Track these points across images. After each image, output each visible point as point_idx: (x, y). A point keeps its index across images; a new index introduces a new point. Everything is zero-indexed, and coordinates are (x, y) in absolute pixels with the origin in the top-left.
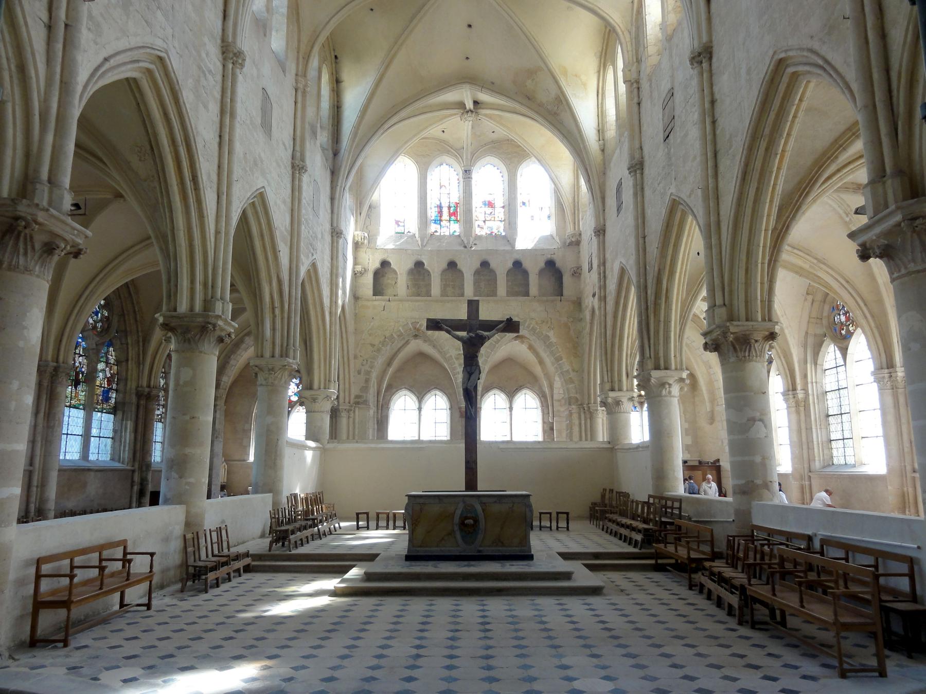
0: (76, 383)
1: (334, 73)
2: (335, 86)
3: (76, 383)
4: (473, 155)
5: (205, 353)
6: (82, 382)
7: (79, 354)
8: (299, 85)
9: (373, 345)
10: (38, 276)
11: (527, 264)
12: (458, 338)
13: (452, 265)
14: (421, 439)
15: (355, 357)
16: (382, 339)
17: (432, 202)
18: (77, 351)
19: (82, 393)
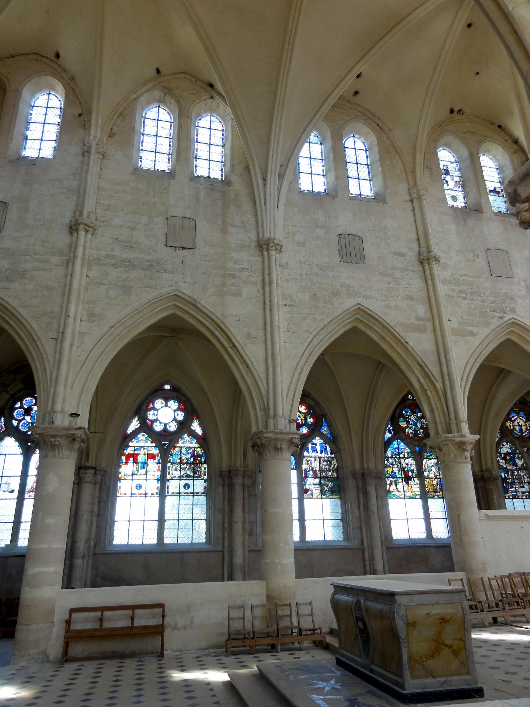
0: (407, 479)
1: (507, 138)
2: (515, 146)
3: (407, 479)
5: (268, 460)
6: (413, 478)
7: (404, 457)
8: (412, 196)
10: (51, 458)
18: (402, 456)
19: (415, 486)
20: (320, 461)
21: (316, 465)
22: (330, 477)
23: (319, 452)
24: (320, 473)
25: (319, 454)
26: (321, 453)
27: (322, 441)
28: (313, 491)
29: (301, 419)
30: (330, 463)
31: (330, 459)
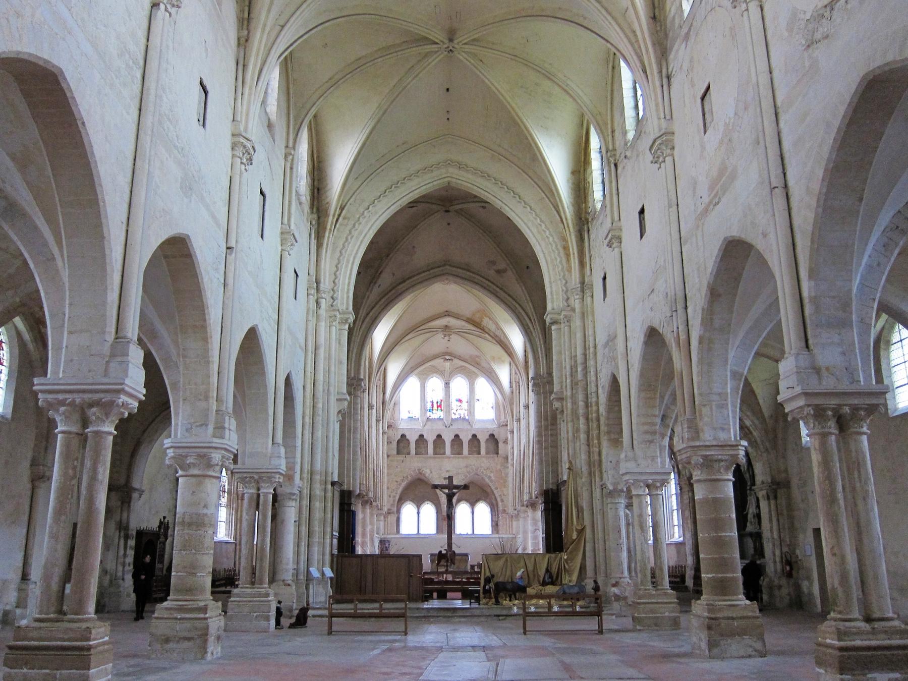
4: (450, 373)
9: (397, 482)
11: (479, 437)
12: (444, 493)
13: (439, 436)
14: (421, 532)
15: (388, 488)
16: (402, 478)
17: (429, 400)
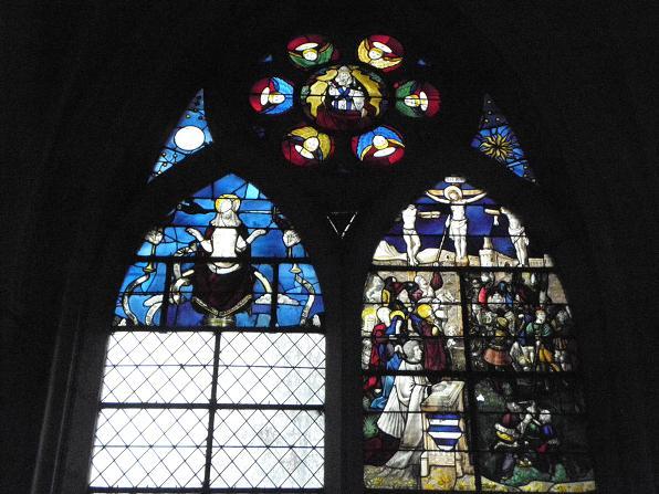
20: (466, 290)
21: (444, 312)
22: (531, 375)
23: (461, 245)
24: (467, 353)
25: (460, 256)
26: (473, 247)
27: (479, 195)
28: (420, 448)
29: (367, 97)
30: (526, 298)
31: (529, 279)
